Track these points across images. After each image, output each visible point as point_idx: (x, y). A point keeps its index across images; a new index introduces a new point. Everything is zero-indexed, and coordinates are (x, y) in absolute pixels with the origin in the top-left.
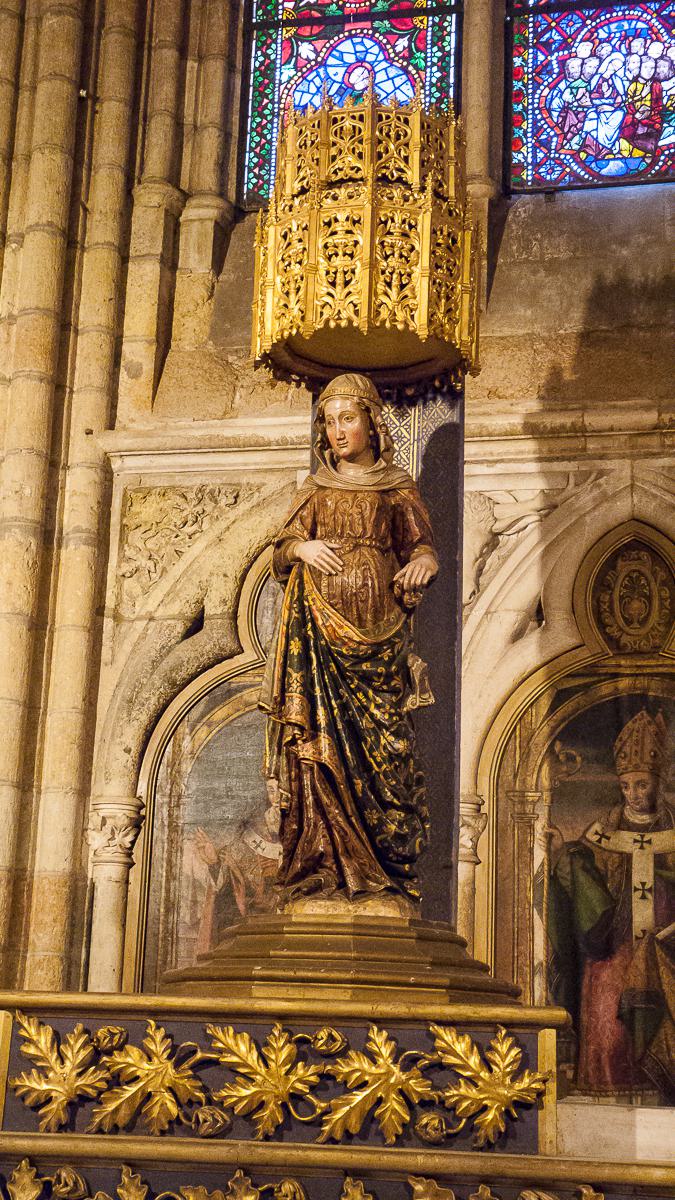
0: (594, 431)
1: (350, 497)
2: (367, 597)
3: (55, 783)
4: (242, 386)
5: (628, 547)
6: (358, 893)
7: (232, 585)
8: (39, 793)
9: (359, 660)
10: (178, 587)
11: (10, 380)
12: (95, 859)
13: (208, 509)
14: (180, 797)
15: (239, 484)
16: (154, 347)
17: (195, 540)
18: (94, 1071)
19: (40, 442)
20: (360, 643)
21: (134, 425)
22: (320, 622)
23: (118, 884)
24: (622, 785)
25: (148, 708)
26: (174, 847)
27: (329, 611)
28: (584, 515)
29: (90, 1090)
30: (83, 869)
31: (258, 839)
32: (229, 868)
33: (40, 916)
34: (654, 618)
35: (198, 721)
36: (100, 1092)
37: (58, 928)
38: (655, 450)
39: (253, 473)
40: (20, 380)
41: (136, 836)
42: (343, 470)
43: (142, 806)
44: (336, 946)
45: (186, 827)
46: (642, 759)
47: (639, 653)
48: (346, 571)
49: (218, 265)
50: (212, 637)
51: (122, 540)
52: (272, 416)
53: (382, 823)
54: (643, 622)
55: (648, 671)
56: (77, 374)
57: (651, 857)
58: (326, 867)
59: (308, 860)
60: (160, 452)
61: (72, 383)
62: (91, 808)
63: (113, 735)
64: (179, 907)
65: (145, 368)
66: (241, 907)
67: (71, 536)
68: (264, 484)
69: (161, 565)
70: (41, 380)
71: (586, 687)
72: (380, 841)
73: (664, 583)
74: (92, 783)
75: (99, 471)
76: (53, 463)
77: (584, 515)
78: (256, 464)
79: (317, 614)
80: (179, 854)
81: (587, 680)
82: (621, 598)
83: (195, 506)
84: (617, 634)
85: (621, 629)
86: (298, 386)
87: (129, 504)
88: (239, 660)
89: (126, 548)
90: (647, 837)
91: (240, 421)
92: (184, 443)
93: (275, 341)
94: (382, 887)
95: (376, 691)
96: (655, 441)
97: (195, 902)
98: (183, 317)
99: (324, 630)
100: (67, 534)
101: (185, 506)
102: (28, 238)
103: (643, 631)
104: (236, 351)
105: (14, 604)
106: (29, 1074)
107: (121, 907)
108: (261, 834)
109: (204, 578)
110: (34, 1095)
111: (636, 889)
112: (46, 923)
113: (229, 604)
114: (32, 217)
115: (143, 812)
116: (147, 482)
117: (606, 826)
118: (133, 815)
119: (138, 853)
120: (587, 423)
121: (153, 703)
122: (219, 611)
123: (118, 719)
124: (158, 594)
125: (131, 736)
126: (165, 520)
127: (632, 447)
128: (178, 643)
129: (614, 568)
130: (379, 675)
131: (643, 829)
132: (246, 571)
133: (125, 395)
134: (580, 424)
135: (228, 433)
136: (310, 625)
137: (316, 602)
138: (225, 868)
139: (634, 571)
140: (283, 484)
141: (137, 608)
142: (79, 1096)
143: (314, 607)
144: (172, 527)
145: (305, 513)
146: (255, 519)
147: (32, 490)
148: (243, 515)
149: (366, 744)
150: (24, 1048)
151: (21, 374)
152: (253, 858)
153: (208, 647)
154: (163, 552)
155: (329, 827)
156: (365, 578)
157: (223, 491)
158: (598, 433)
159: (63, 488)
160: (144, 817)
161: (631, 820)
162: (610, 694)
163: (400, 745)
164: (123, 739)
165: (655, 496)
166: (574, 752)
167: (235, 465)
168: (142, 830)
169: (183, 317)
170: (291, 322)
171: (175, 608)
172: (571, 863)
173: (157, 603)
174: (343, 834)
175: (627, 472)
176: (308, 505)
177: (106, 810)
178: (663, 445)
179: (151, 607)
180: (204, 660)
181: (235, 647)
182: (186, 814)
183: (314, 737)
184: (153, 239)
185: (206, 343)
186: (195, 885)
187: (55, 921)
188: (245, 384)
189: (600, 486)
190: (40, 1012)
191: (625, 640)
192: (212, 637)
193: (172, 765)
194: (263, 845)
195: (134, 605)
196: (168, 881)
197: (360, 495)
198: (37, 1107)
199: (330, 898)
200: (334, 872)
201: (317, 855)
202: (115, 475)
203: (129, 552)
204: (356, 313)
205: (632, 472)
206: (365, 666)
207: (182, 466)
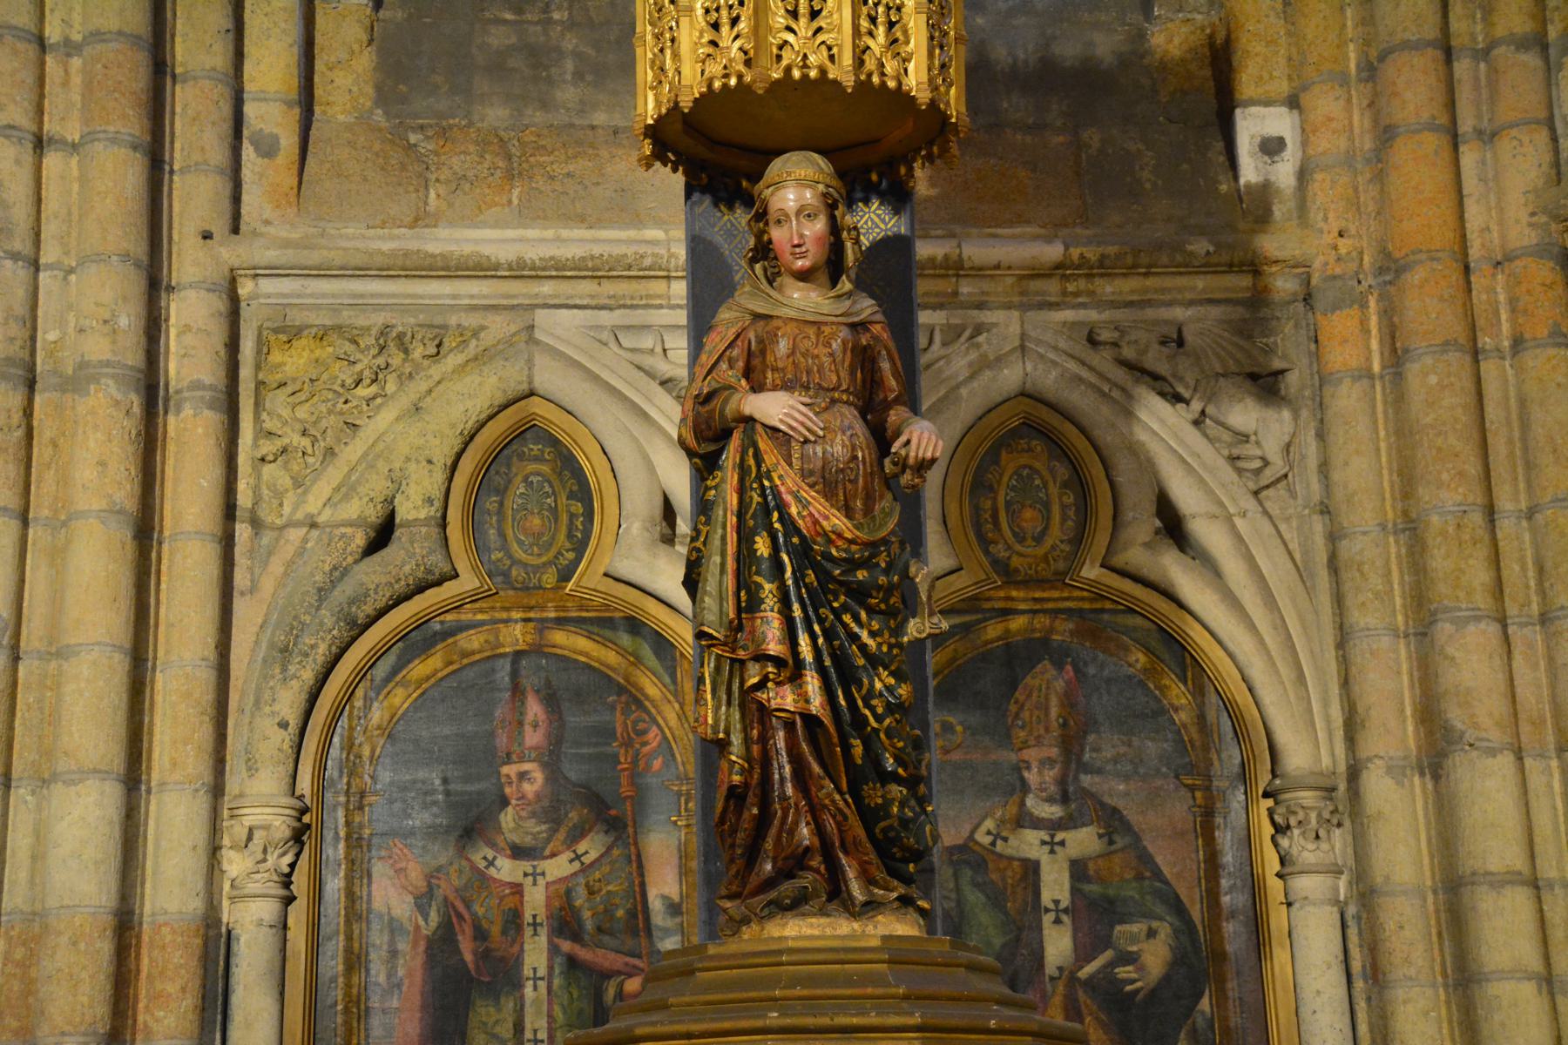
0: (972, 268)
1: (811, 331)
2: (857, 475)
3: (177, 776)
4: (437, 180)
5: (1014, 433)
6: (866, 904)
7: (439, 476)
8: (149, 791)
9: (852, 564)
10: (353, 478)
11: (75, 147)
12: (235, 893)
14: (362, 794)
15: (445, 327)
16: (297, 111)
17: (379, 407)
19: (140, 250)
20: (851, 542)
21: (271, 230)
22: (794, 510)
23: (274, 930)
24: (1022, 765)
25: (315, 661)
26: (358, 872)
27: (808, 494)
28: (958, 387)
31: (490, 854)
32: (446, 899)
33: (159, 986)
34: (1056, 534)
35: (388, 679)
38: (1053, 299)
40: (99, 146)
41: (298, 855)
42: (788, 292)
43: (304, 811)
44: (866, 980)
45: (375, 840)
46: (1047, 730)
47: (1041, 583)
48: (829, 436)
50: (402, 559)
51: (258, 405)
52: (491, 227)
53: (888, 803)
54: (1039, 539)
55: (1050, 605)
56: (177, 145)
57: (1066, 865)
58: (810, 868)
59: (786, 858)
61: (172, 157)
62: (226, 813)
63: (257, 703)
64: (368, 961)
65: (283, 142)
66: (468, 957)
67: (186, 394)
68: (483, 328)
69: (322, 444)
70: (135, 148)
71: (966, 628)
72: (884, 830)
73: (1065, 485)
74: (227, 773)
75: (224, 296)
77: (958, 387)
78: (472, 297)
79: (788, 498)
80: (365, 881)
81: (967, 618)
82: (1008, 504)
83: (374, 357)
84: (1004, 554)
85: (1009, 548)
86: (675, 170)
87: (265, 350)
88: (449, 590)
89: (264, 416)
90: (1059, 837)
91: (443, 232)
92: (359, 260)
93: (697, 96)
94: (895, 895)
95: (871, 611)
96: (1052, 287)
97: (394, 953)
99: (800, 522)
101: (359, 356)
103: (1041, 551)
104: (422, 128)
105: (111, 496)
107: (277, 964)
108: (493, 845)
109: (397, 465)
111: (1047, 910)
112: (170, 995)
113: (438, 504)
115: (306, 819)
116: (296, 318)
117: (1001, 822)
118: (296, 824)
120: (965, 256)
121: (322, 652)
122: (422, 515)
125: (288, 703)
126: (325, 377)
127: (1022, 294)
128: (356, 562)
129: (997, 463)
130: (879, 588)
131: (1055, 826)
133: (253, 183)
134: (955, 257)
135: (432, 248)
136: (776, 515)
137: (787, 480)
138: (440, 899)
139: (1025, 467)
140: (513, 328)
141: (287, 509)
143: (782, 489)
145: (735, 352)
146: (471, 380)
147: (129, 319)
148: (453, 372)
149: (859, 690)
151: (101, 136)
152: (482, 879)
153: (407, 569)
154: (324, 423)
155: (815, 811)
156: (854, 448)
157: (419, 337)
158: (979, 272)
159: (167, 320)
161: (1036, 813)
162: (999, 639)
163: (903, 691)
164: (277, 707)
165: (1054, 363)
166: (951, 719)
168: (306, 848)
170: (725, 67)
171: (353, 509)
172: (956, 876)
173: (324, 500)
174: (839, 818)
175: (1015, 329)
176: (739, 343)
177: (253, 816)
178: (1064, 293)
179: (313, 505)
180: (400, 588)
181: (447, 568)
183: (796, 677)
186: (394, 927)
187: (183, 990)
188: (442, 177)
189: (978, 346)
191: (1016, 562)
192: (402, 559)
193: (349, 745)
194: (498, 862)
195: (281, 505)
196: (348, 922)
197: (827, 330)
199: (823, 913)
200: (822, 876)
201: (800, 850)
202: (243, 305)
203: (269, 425)
204: (832, 58)
205: (1022, 327)
206: (861, 575)
207: (355, 296)
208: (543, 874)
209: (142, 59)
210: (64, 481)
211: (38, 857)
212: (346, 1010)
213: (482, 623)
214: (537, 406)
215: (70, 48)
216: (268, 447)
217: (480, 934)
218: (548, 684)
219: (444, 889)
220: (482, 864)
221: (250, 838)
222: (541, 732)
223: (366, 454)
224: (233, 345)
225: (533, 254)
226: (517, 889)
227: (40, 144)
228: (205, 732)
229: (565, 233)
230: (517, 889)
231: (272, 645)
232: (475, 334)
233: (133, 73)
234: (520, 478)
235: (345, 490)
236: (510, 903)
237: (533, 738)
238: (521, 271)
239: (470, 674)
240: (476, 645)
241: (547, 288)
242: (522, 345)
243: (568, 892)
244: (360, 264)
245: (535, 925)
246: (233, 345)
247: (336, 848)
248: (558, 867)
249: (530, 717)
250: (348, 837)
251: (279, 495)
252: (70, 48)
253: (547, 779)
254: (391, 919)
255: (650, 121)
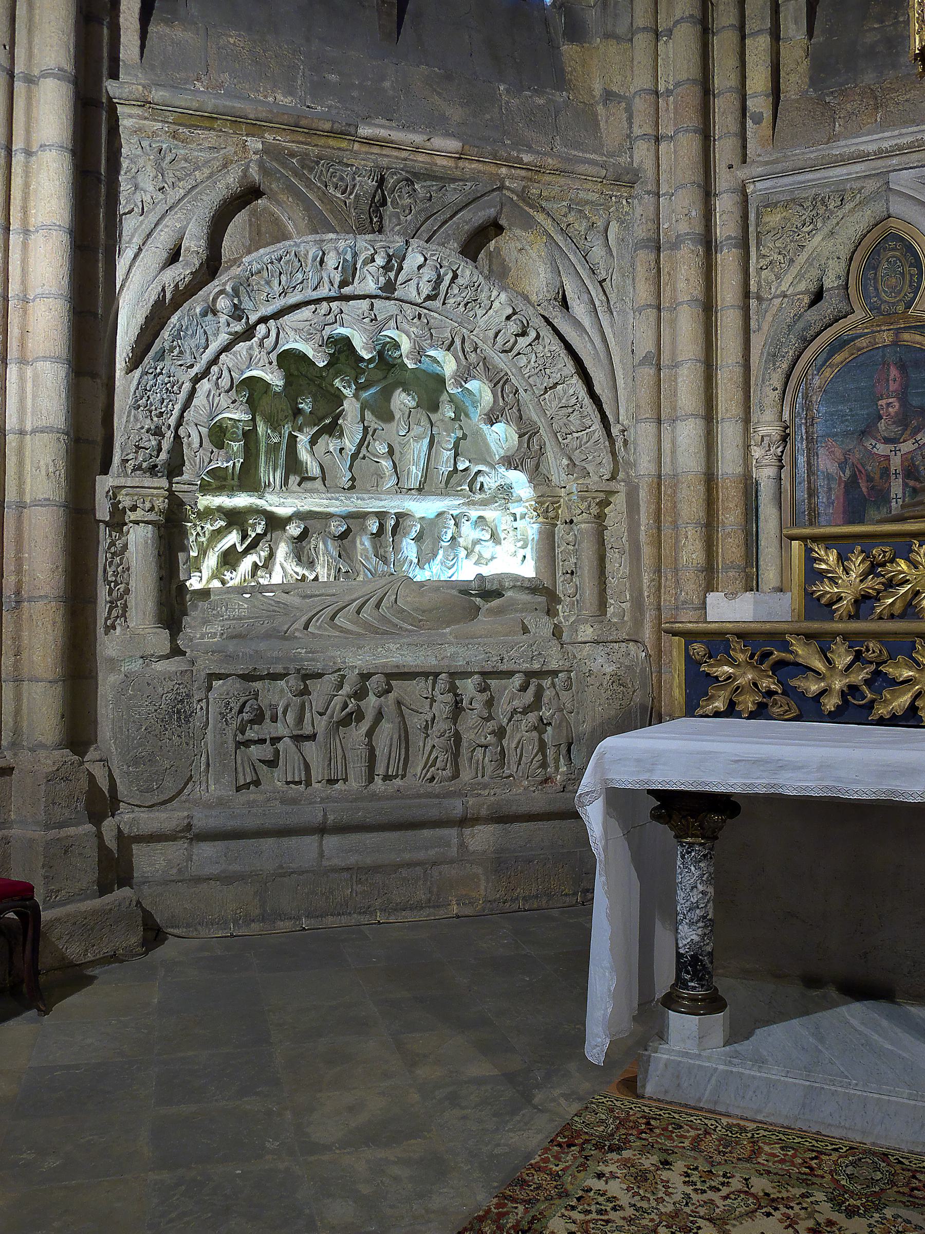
7: (843, 264)
13: (820, 212)
15: (844, 190)
16: (771, 99)
18: (873, 578)
19: (699, 178)
21: (761, 158)
25: (788, 359)
26: (811, 453)
29: (870, 591)
30: (750, 472)
36: (878, 593)
37: (739, 511)
39: (854, 180)
40: (680, 135)
41: (785, 447)
49: (810, 33)
50: (828, 307)
52: (868, 135)
60: (784, 174)
61: (714, 134)
63: (763, 380)
67: (724, 243)
68: (863, 187)
76: (708, 194)
78: (857, 173)
91: (842, 143)
92: (800, 164)
97: (830, 489)
98: (788, 74)
100: (720, 243)
101: (804, 212)
102: (675, 31)
104: (832, 92)
106: (822, 582)
108: (875, 438)
110: (828, 596)
114: (678, 14)
115: (788, 431)
119: (786, 460)
123: (766, 368)
124: (789, 278)
125: (776, 380)
128: (806, 311)
132: (853, 253)
141: (773, 290)
142: (862, 595)
144: (793, 229)
150: (815, 565)
154: (789, 248)
159: (715, 210)
160: (789, 434)
167: (841, 176)
169: (788, 74)
171: (802, 287)
177: (763, 430)
180: (826, 320)
182: (819, 429)
184: (763, 18)
185: (807, 91)
186: (829, 477)
190: (828, 540)
192: (828, 307)
193: (806, 397)
195: (770, 289)
198: (830, 604)
208: (900, 450)
209: (697, 90)
210: (674, 290)
211: (673, 452)
212: (809, 514)
213: (867, 333)
214: (892, 222)
215: (669, 92)
216: (763, 262)
217: (870, 479)
218: (901, 359)
219: (852, 459)
220: (870, 447)
221: (762, 440)
222: (897, 383)
223: (808, 259)
224: (745, 217)
225: (885, 145)
226: (887, 458)
227: (657, 140)
228: (739, 395)
229: (904, 131)
230: (887, 458)
231: (769, 354)
232: (860, 192)
233: (692, 96)
234: (885, 259)
235: (800, 276)
236: (884, 465)
237: (893, 386)
238: (881, 155)
239: (863, 358)
240: (865, 345)
241: (895, 161)
242: (883, 193)
243: (912, 458)
244: (801, 167)
245: (896, 474)
246: (745, 217)
247: (802, 444)
248: (907, 447)
249: (892, 377)
250: (807, 438)
251: (769, 284)
252: (669, 92)
253: (900, 406)
254: (828, 474)
255: (917, 52)
